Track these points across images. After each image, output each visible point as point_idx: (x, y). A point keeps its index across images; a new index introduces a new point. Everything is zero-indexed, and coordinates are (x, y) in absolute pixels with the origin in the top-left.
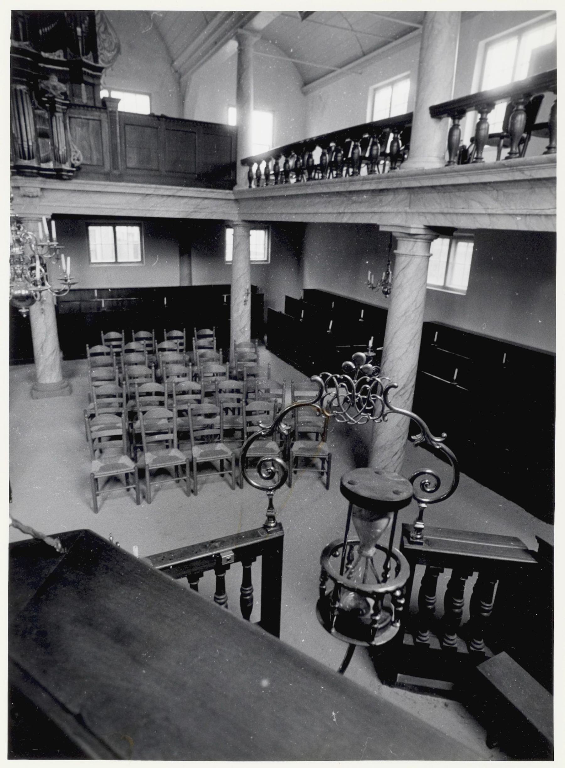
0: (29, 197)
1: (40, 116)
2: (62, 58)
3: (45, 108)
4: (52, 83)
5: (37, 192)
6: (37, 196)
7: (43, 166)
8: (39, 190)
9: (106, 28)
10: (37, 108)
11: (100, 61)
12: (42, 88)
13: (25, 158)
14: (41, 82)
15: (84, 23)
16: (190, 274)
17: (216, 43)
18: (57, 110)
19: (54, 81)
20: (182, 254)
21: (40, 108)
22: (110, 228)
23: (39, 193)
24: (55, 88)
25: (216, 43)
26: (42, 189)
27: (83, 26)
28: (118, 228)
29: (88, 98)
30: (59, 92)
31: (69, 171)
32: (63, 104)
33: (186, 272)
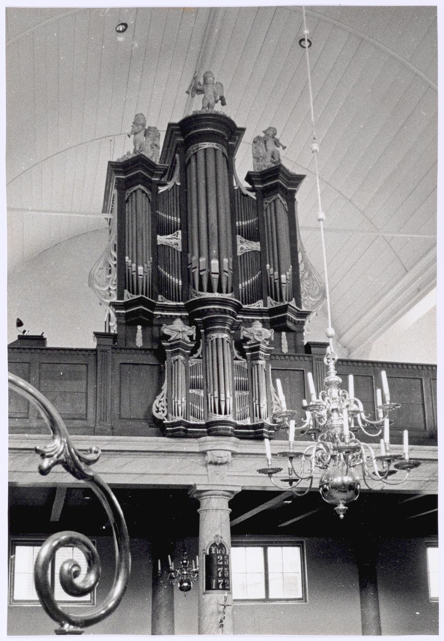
0: (216, 464)
1: (239, 367)
2: (262, 307)
3: (245, 357)
4: (257, 329)
5: (226, 457)
6: (226, 463)
7: (239, 423)
8: (230, 453)
9: (310, 275)
10: (236, 359)
11: (303, 307)
12: (244, 337)
13: (220, 413)
14: (243, 330)
15: (288, 271)
16: (378, 616)
17: (419, 290)
18: (260, 357)
19: (258, 326)
20: (363, 587)
21: (240, 358)
22: (260, 550)
23: (230, 458)
24: (260, 334)
25: (419, 290)
26: (234, 454)
27: (288, 273)
28: (270, 550)
29: (289, 348)
30: (263, 339)
31: (270, 428)
32: (268, 351)
33: (372, 613)
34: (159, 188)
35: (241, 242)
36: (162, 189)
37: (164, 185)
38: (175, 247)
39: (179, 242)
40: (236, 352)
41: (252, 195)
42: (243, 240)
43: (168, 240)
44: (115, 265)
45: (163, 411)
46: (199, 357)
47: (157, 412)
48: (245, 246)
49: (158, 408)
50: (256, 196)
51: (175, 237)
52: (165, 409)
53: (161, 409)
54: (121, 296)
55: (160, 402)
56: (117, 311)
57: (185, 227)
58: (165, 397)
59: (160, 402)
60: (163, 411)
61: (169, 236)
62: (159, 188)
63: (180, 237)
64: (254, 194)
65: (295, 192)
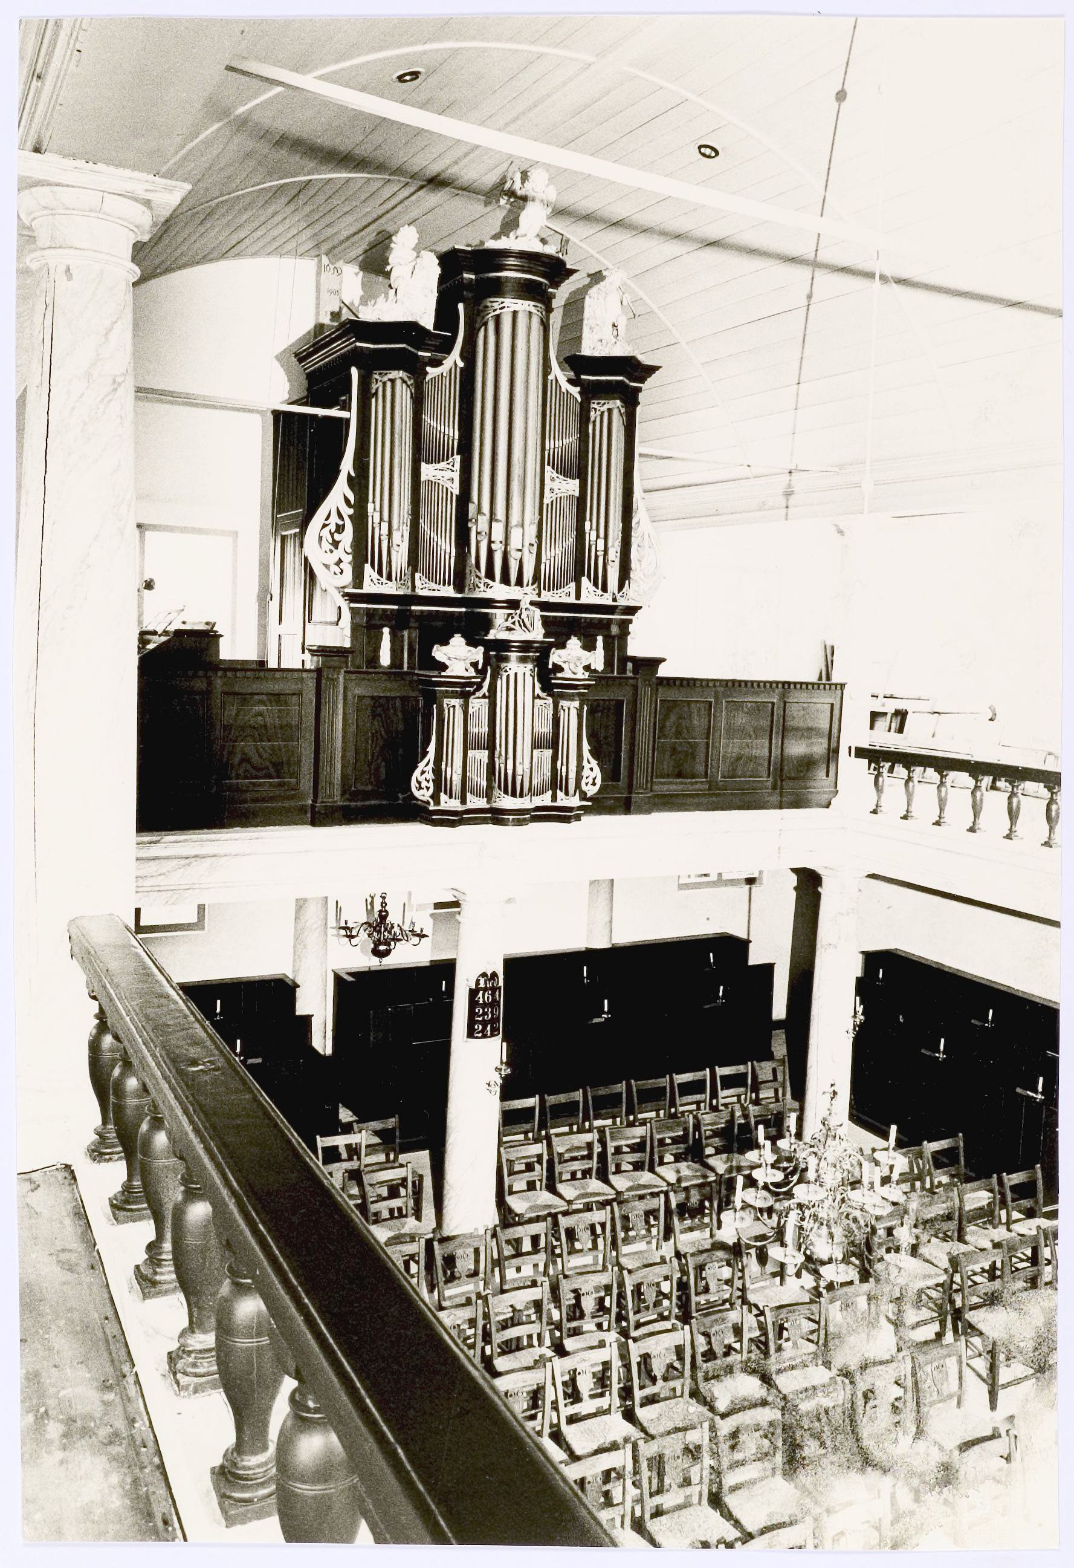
10: (539, 697)
21: (543, 695)
34: (428, 369)
35: (552, 479)
36: (432, 372)
37: (437, 363)
38: (448, 484)
39: (456, 476)
40: (538, 685)
41: (575, 391)
42: (555, 475)
43: (439, 474)
44: (350, 517)
45: (428, 788)
46: (484, 697)
47: (420, 788)
48: (555, 485)
49: (419, 783)
50: (580, 393)
51: (450, 467)
52: (431, 785)
53: (424, 784)
54: (358, 578)
55: (423, 772)
56: (352, 605)
57: (465, 448)
58: (431, 765)
59: (423, 772)
60: (428, 788)
61: (443, 465)
62: (428, 369)
63: (457, 466)
64: (578, 389)
65: (639, 390)
